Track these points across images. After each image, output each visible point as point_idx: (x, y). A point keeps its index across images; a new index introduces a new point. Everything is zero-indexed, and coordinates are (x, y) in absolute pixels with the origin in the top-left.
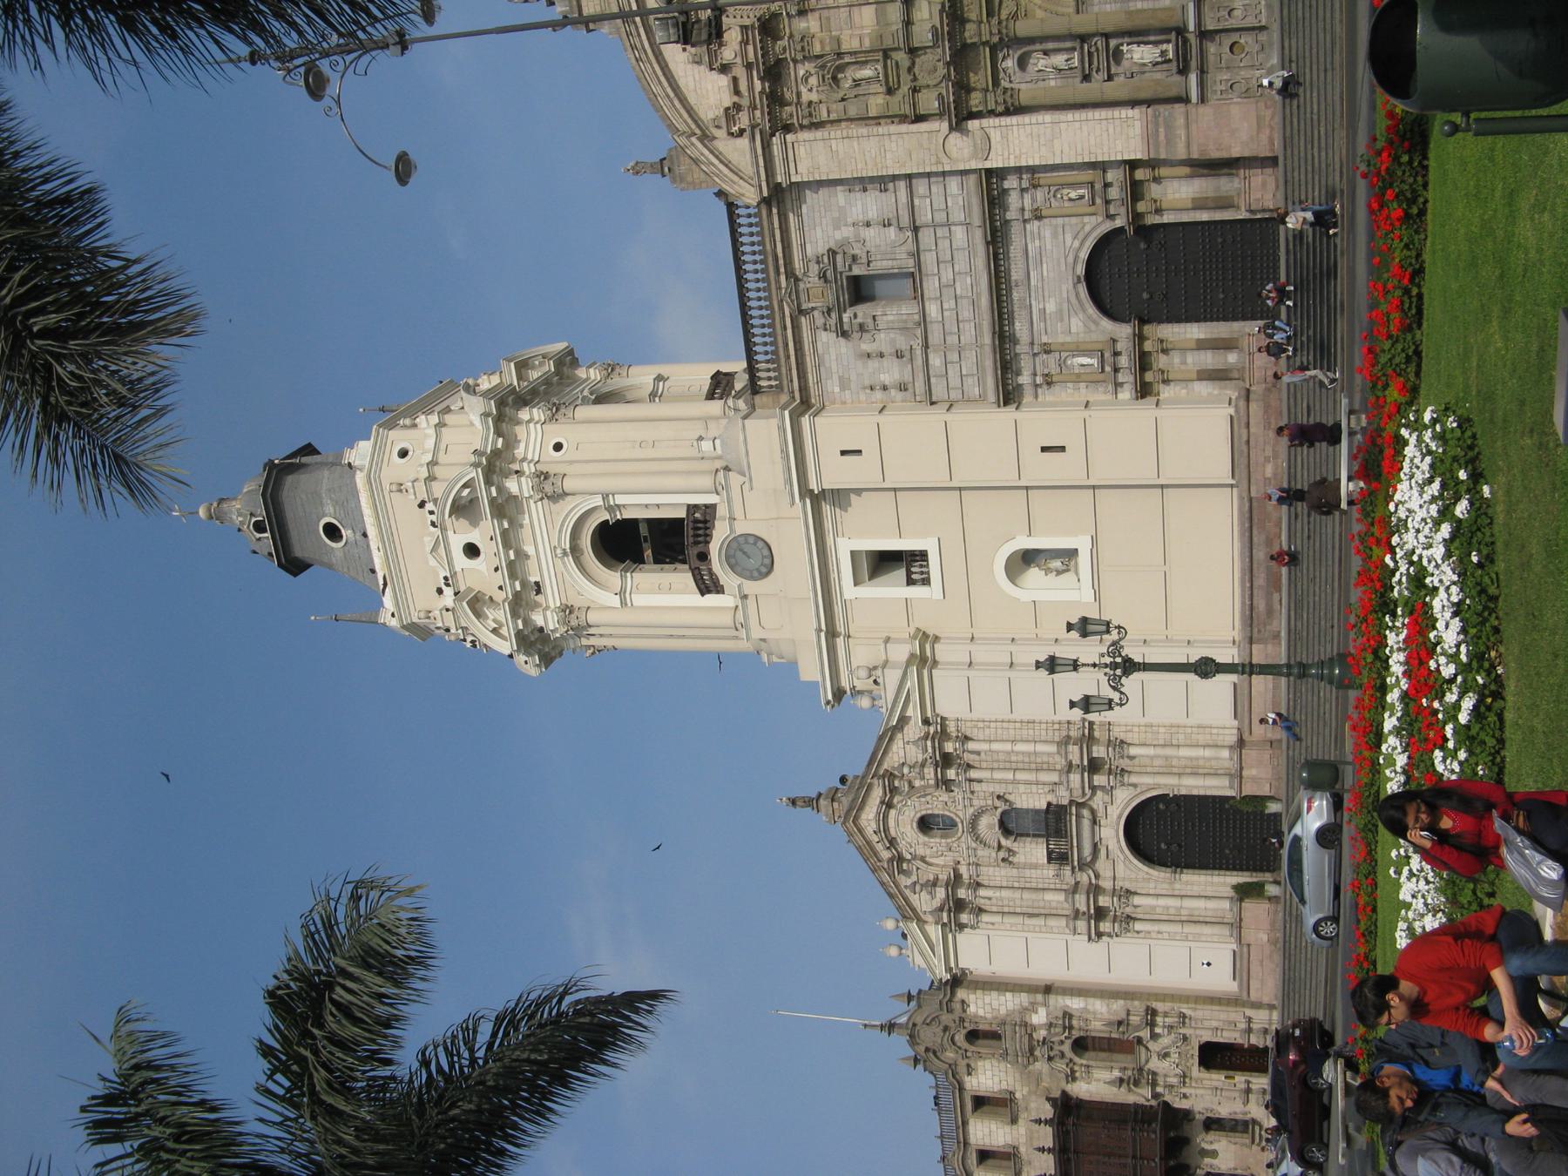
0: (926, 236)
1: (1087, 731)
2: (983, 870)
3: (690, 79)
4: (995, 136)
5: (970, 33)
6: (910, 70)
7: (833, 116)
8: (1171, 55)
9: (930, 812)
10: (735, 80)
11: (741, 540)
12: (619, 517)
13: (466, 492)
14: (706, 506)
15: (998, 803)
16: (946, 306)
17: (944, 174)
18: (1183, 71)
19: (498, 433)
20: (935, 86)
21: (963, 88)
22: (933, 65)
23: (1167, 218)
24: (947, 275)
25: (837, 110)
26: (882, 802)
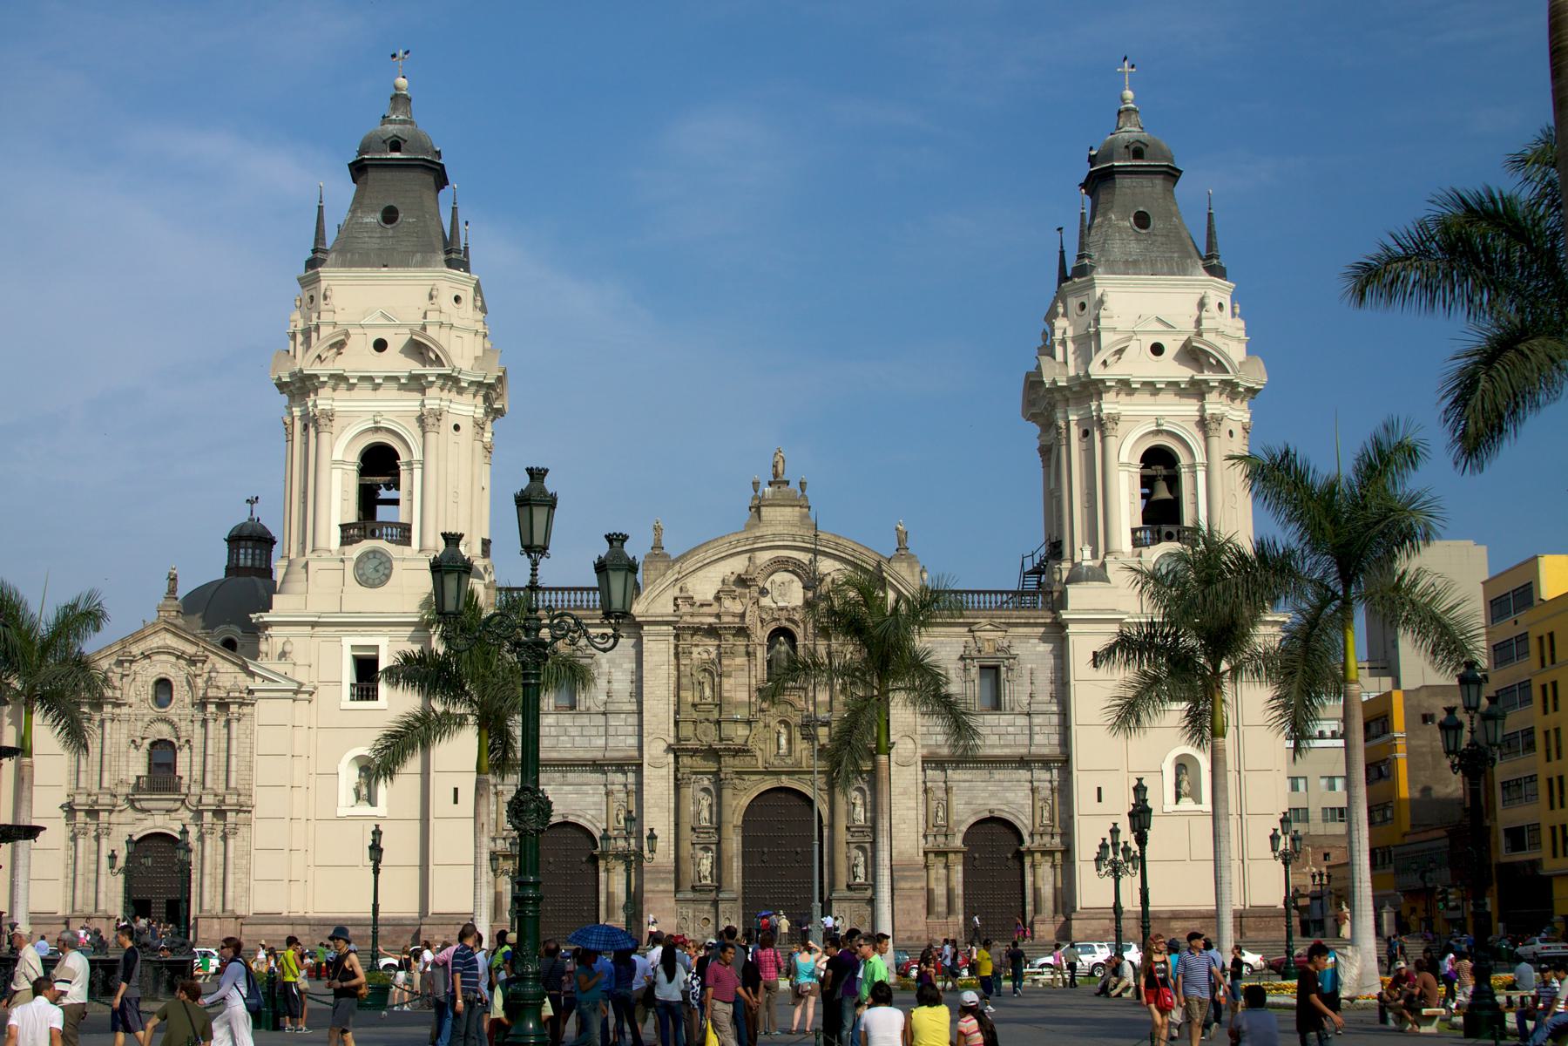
0: (600, 720)
1: (245, 808)
2: (125, 726)
3: (714, 575)
4: (664, 771)
5: (727, 761)
6: (707, 720)
7: (682, 668)
8: (704, 882)
9: (175, 688)
10: (710, 605)
11: (387, 565)
12: (402, 468)
13: (433, 357)
14: (410, 537)
15: (183, 740)
16: (552, 729)
17: (640, 736)
18: (694, 888)
19: (471, 383)
20: (696, 735)
21: (694, 752)
22: (710, 737)
23: (602, 875)
24: (574, 731)
25: (685, 670)
26: (183, 653)
